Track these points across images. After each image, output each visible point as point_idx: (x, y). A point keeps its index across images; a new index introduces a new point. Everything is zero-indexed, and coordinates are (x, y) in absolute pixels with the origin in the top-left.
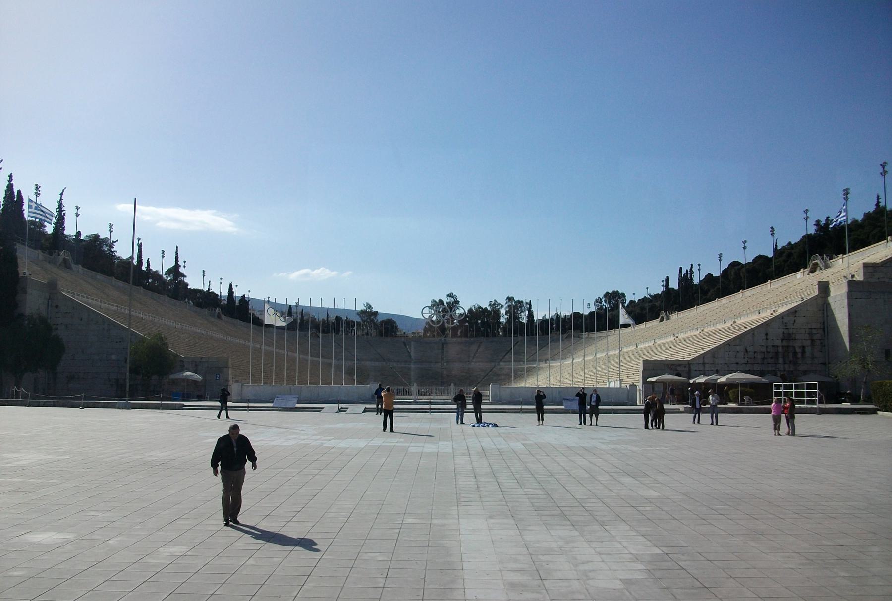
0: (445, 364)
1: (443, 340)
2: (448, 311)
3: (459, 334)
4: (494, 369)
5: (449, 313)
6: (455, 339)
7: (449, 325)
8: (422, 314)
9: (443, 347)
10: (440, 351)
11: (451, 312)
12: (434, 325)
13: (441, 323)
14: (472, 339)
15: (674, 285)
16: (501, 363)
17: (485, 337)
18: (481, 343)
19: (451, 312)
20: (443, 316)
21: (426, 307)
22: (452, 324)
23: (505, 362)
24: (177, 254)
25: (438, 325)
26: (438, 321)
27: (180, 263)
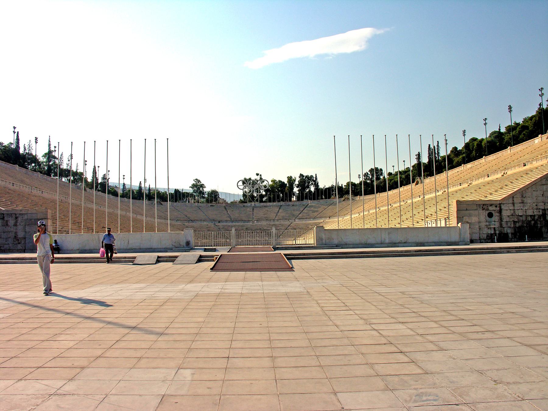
0: (255, 222)
4: (292, 224)
6: (262, 204)
8: (238, 186)
9: (253, 209)
10: (251, 213)
12: (246, 194)
13: (251, 193)
14: (275, 204)
15: (425, 160)
16: (296, 220)
17: (283, 202)
20: (253, 187)
21: (239, 181)
23: (299, 219)
24: (49, 141)
26: (250, 191)
27: (52, 149)
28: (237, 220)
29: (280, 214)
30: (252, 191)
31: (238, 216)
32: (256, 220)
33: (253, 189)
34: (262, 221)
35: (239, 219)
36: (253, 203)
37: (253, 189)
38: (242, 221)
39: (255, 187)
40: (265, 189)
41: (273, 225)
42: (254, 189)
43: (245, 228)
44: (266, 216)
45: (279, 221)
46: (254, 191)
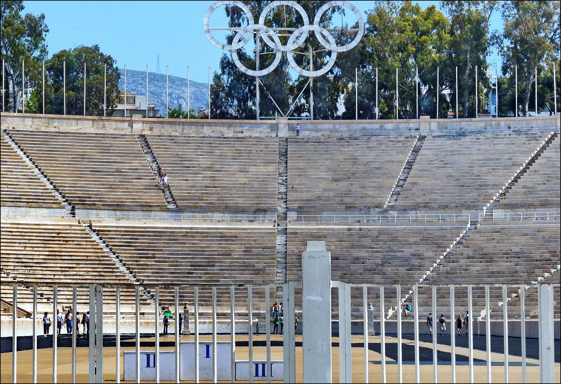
0: (292, 215)
1: (281, 126)
2: (299, 21)
3: (341, 109)
5: (306, 28)
6: (327, 125)
7: (306, 73)
11: (311, 23)
12: (250, 73)
18: (422, 138)
19: (311, 23)
20: (284, 41)
22: (317, 67)
25: (265, 72)
28: (201, 204)
29: (415, 180)
30: (279, 56)
31: (207, 182)
32: (296, 205)
33: (282, 48)
34: (325, 214)
35: (213, 199)
36: (283, 121)
37: (282, 48)
38: (227, 209)
39: (292, 38)
40: (343, 49)
41: (383, 237)
42: (291, 46)
43: (237, 249)
44: (343, 186)
45: (412, 215)
46: (290, 57)
